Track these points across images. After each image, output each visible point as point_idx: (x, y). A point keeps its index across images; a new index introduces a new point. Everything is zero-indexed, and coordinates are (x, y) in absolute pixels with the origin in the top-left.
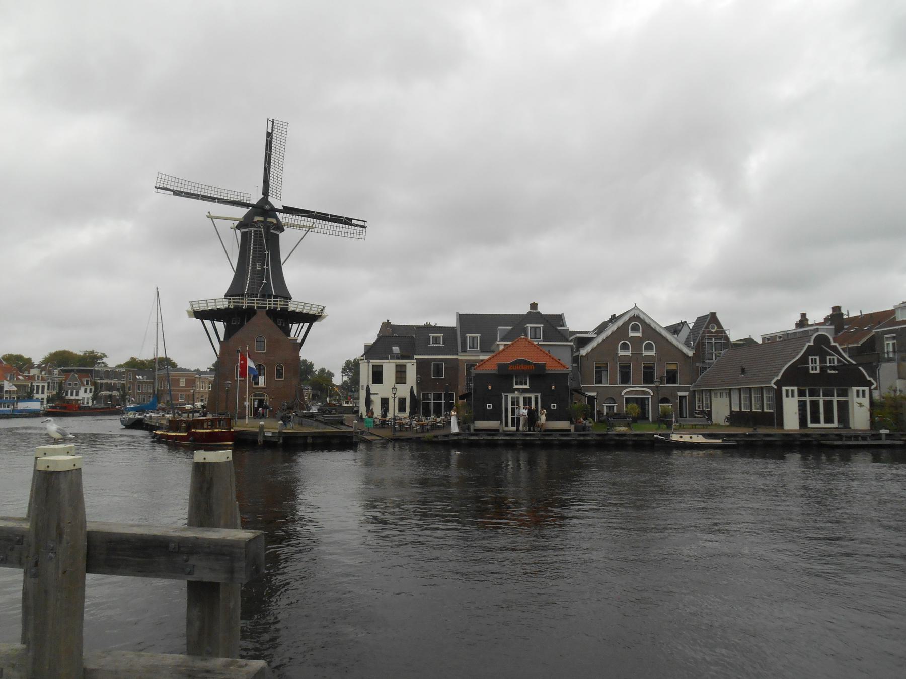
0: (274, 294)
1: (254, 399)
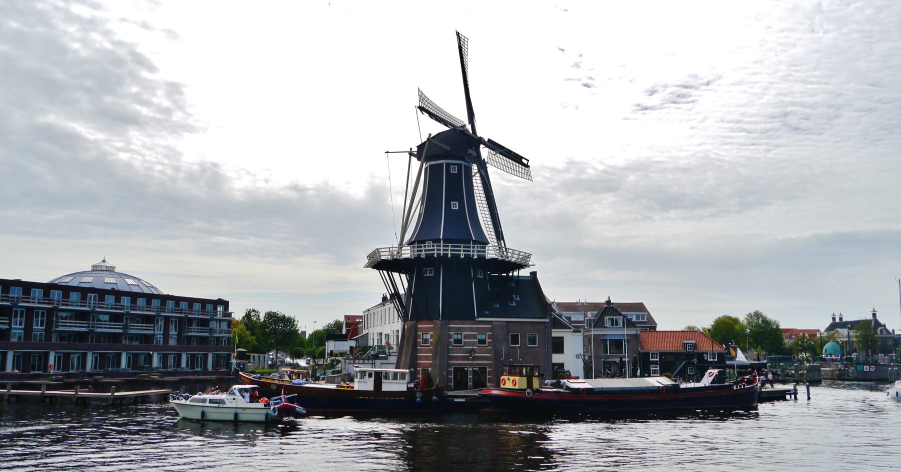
0: (474, 239)
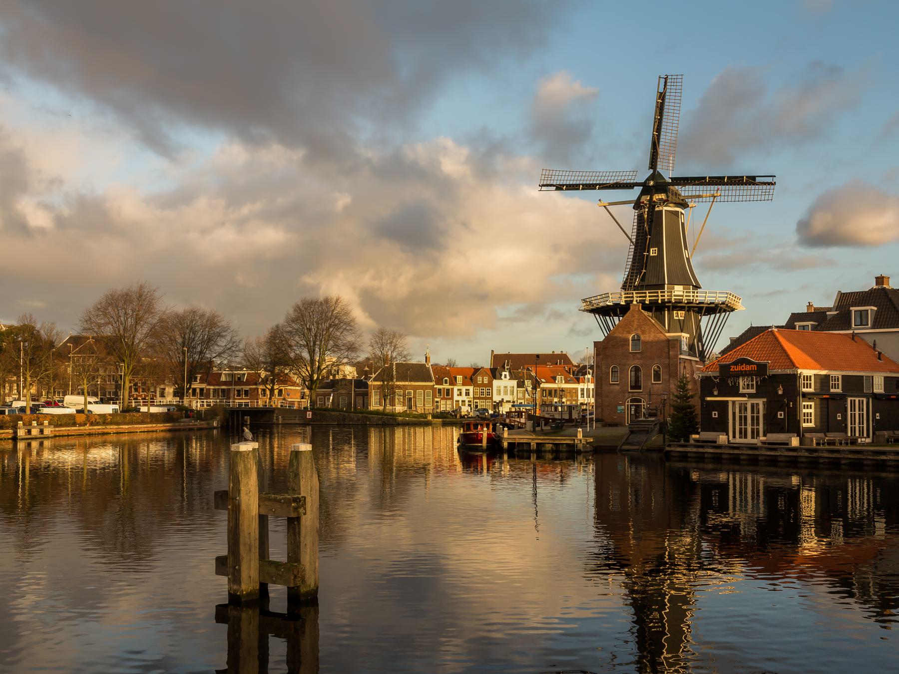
1: (631, 405)
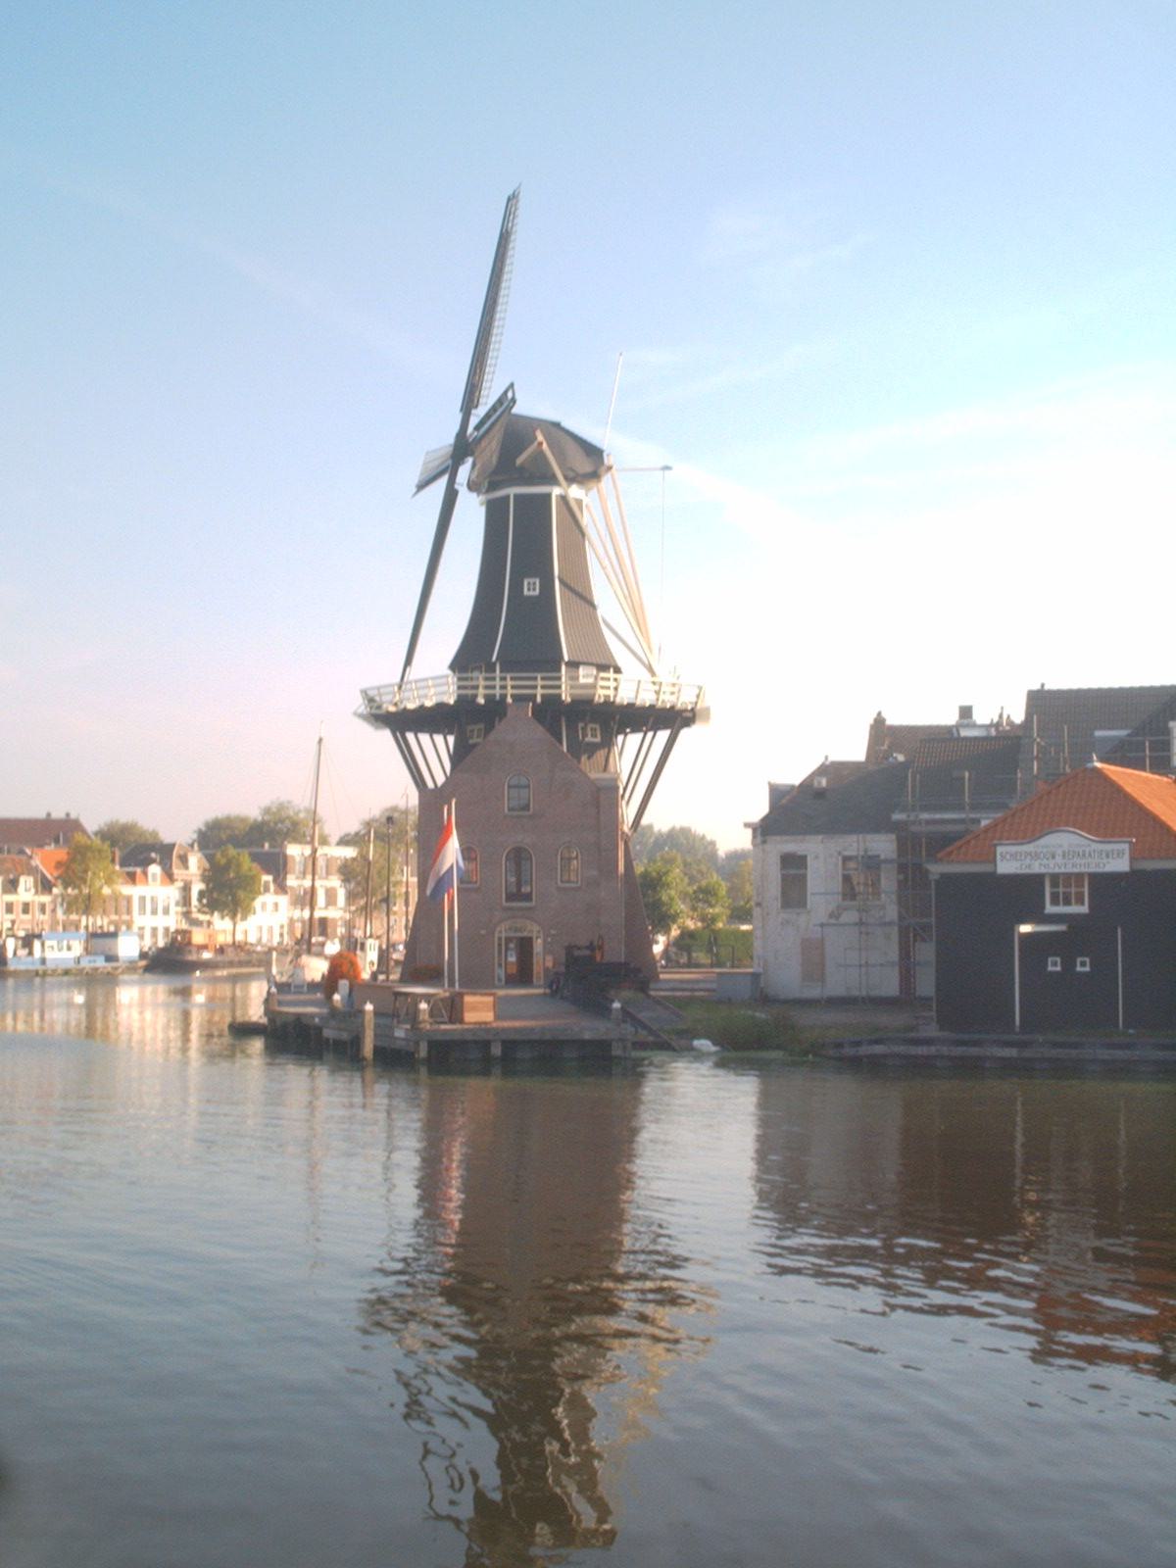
0: (566, 658)
